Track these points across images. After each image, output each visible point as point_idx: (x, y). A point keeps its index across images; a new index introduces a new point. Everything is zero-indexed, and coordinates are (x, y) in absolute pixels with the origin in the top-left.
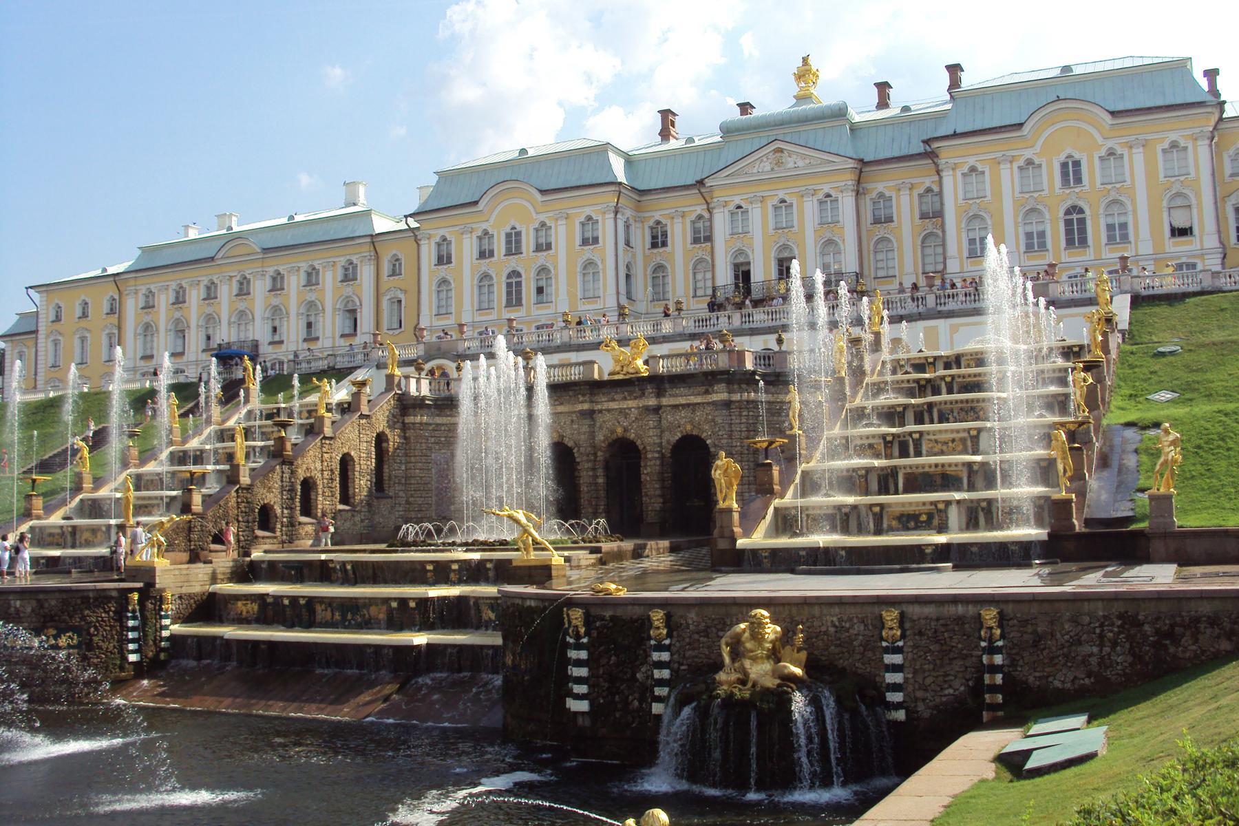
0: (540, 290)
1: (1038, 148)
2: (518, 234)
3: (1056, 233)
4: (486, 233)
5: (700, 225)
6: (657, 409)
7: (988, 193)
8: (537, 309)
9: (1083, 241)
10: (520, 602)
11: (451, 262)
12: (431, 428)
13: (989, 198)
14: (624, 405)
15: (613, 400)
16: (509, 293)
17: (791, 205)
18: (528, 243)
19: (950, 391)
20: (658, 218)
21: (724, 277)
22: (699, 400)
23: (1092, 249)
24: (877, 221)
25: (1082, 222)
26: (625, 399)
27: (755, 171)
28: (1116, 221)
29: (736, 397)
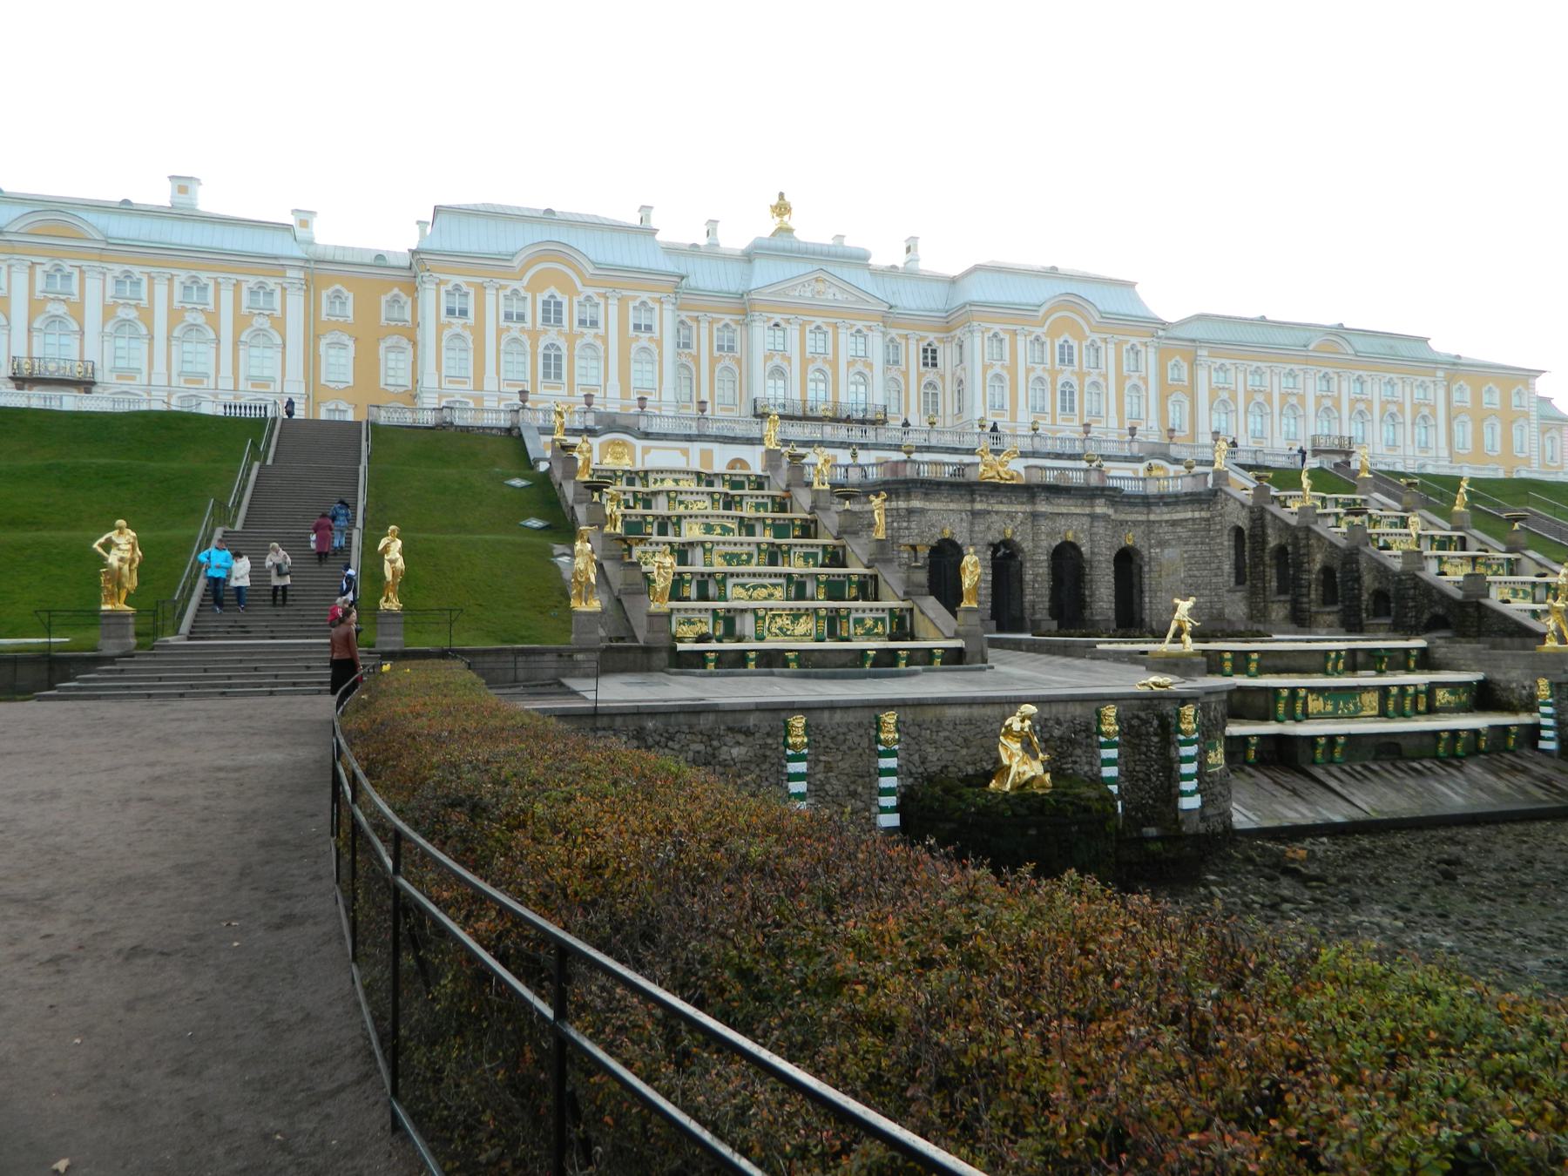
2: (559, 304)
5: (726, 334)
6: (1044, 515)
7: (1007, 356)
9: (1072, 409)
14: (1013, 508)
15: (1001, 503)
16: (546, 366)
17: (825, 333)
18: (571, 312)
22: (1078, 511)
25: (1072, 394)
26: (1011, 503)
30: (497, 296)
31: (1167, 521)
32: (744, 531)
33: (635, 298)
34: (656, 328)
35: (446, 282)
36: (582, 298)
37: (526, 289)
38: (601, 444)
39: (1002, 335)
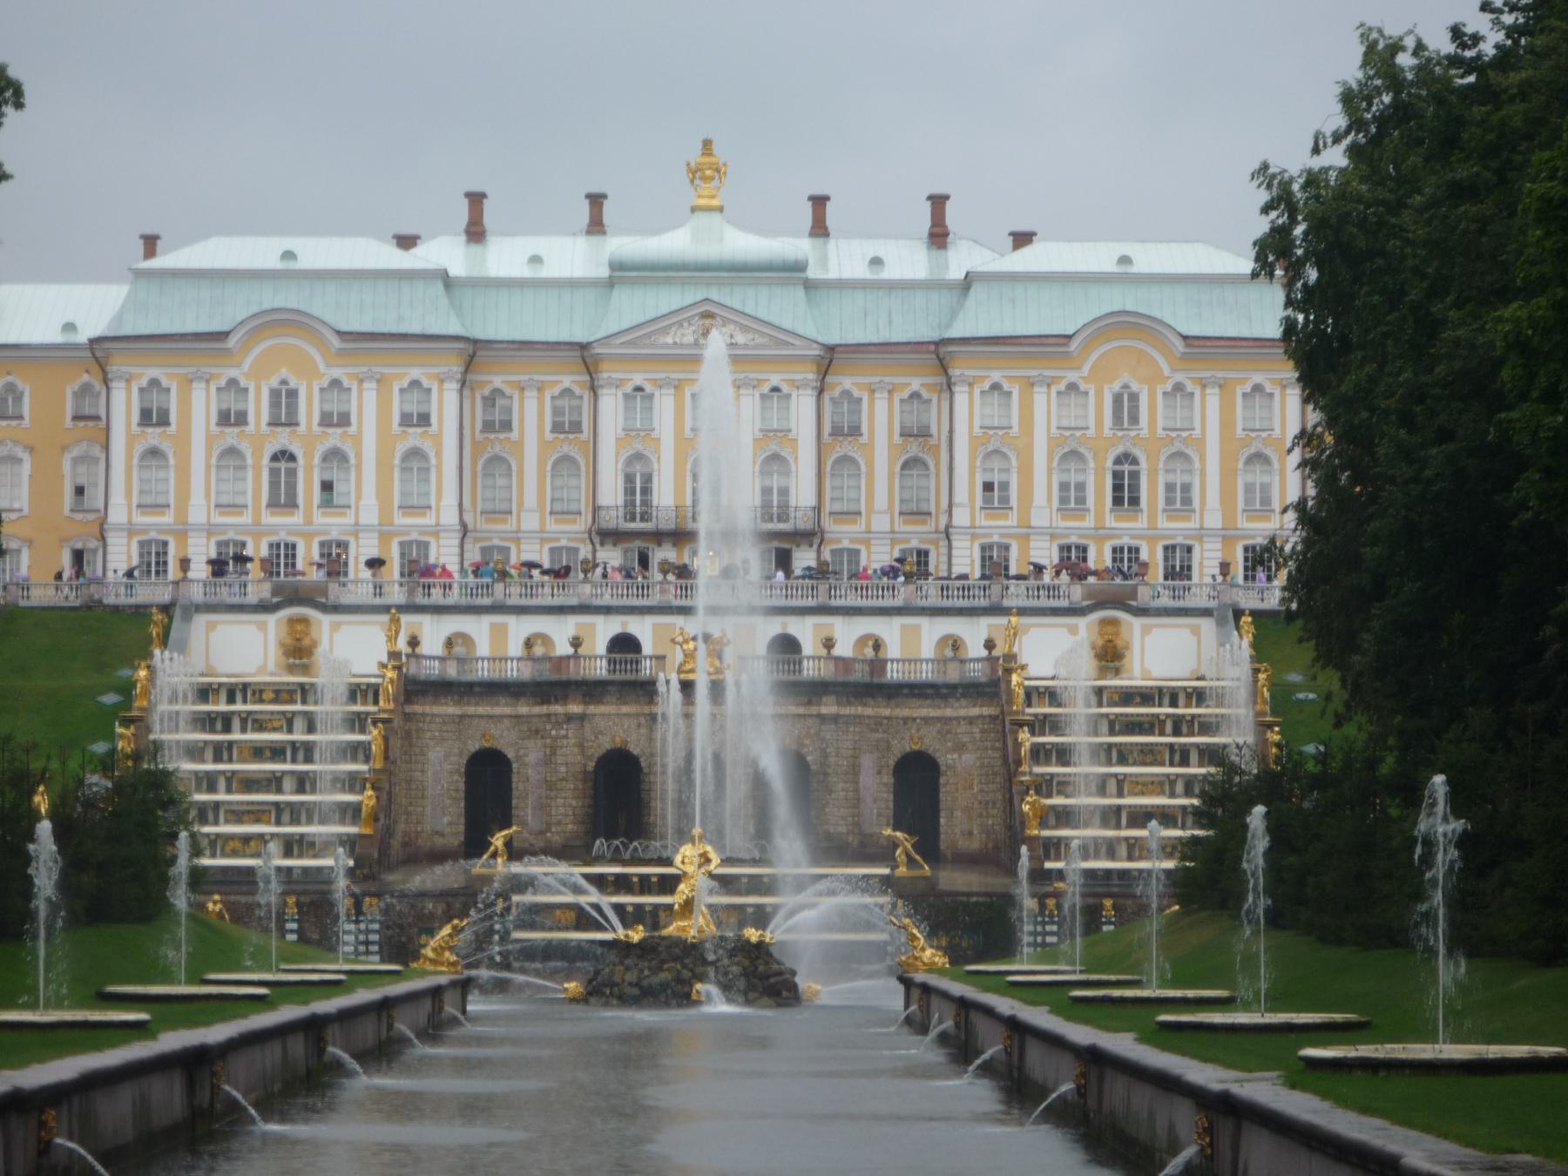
0: (327, 487)
1: (1086, 370)
2: (292, 394)
3: (1099, 489)
4: (233, 382)
5: (565, 403)
8: (324, 514)
9: (1135, 501)
10: (965, 899)
11: (167, 423)
12: (428, 719)
13: (1016, 429)
16: (274, 485)
18: (309, 409)
19: (1112, 732)
20: (498, 381)
21: (611, 493)
23: (1145, 514)
24: (837, 432)
25: (1135, 476)
27: (669, 340)
28: (1179, 479)
29: (847, 711)
30: (208, 389)
31: (964, 718)
32: (301, 755)
33: (402, 376)
34: (434, 419)
35: (140, 376)
36: (326, 385)
37: (247, 375)
38: (278, 622)
39: (1006, 387)
